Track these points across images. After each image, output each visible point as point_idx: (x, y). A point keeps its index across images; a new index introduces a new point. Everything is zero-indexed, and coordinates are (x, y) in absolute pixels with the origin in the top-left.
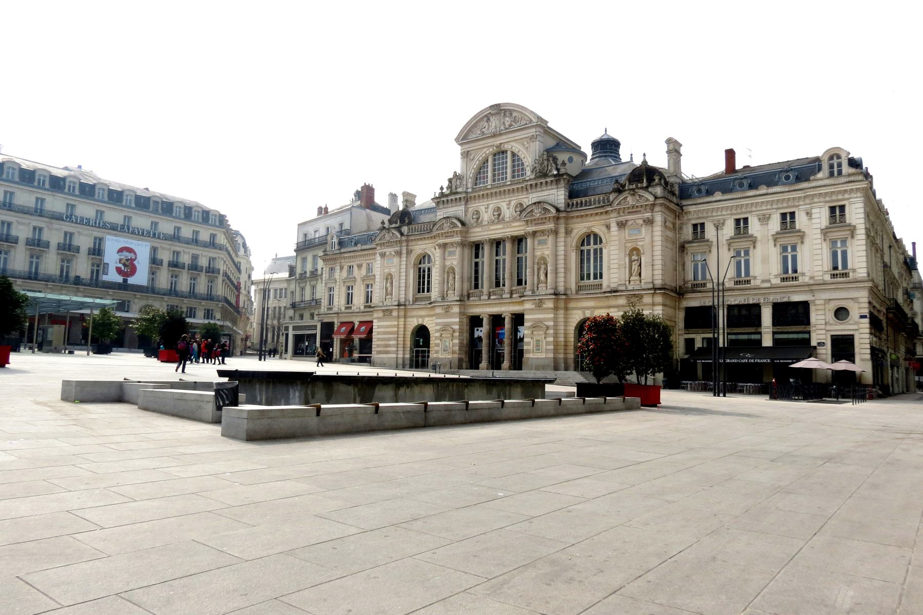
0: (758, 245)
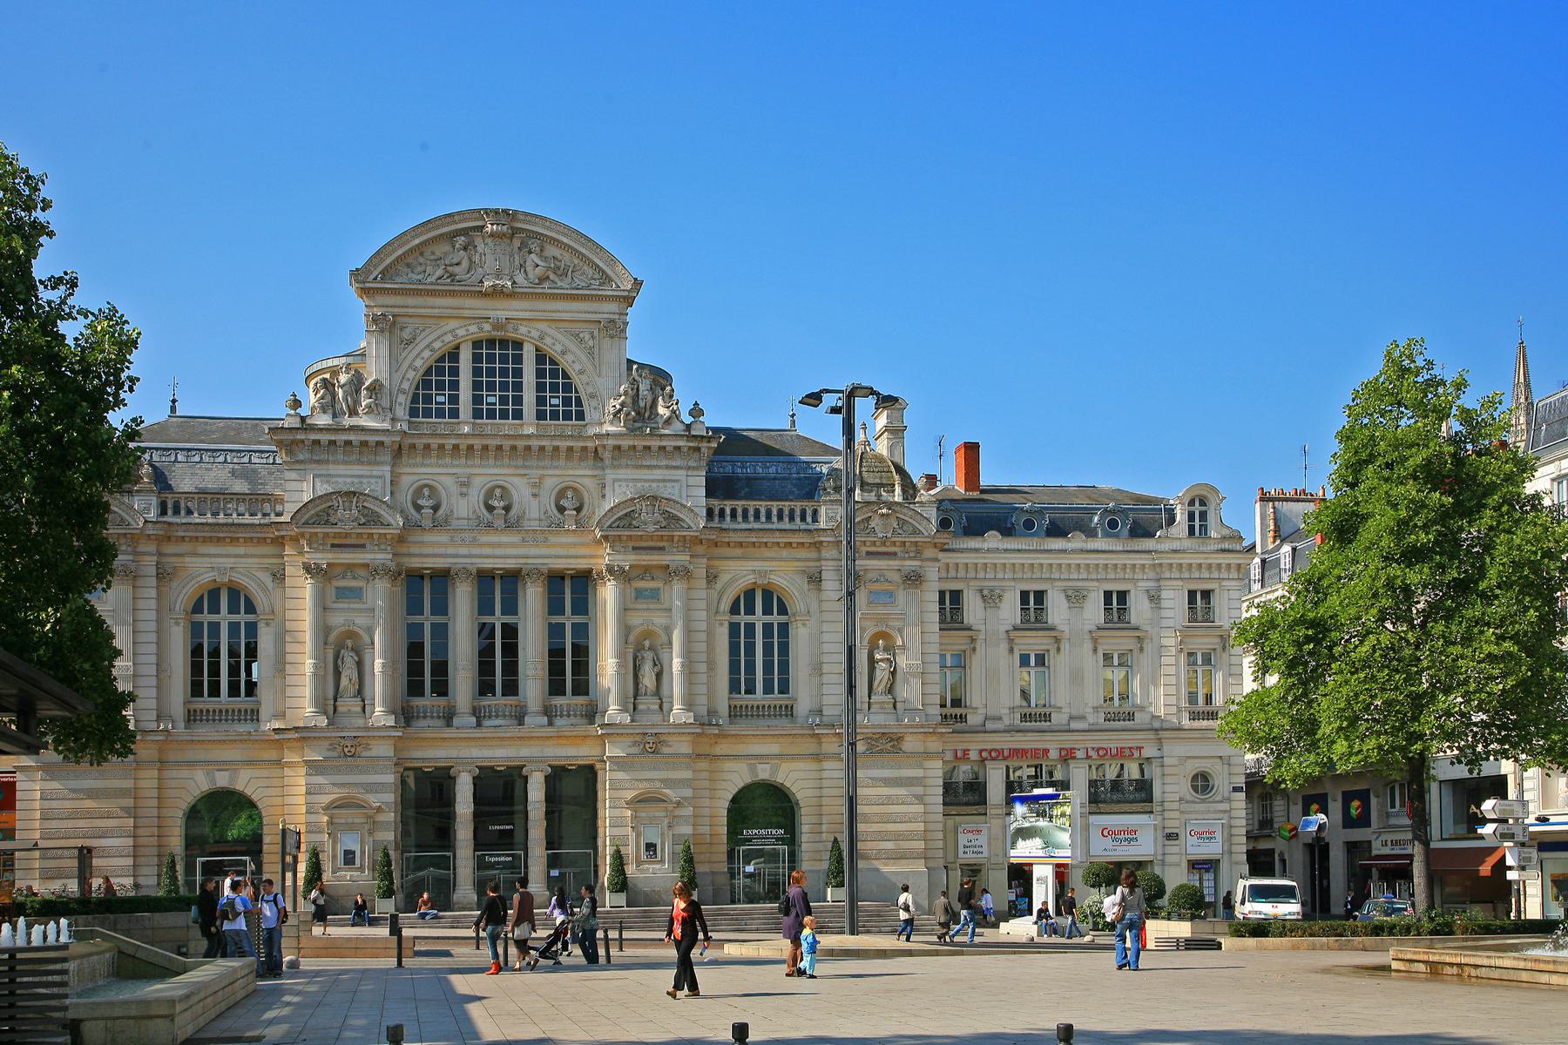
0: (1065, 646)
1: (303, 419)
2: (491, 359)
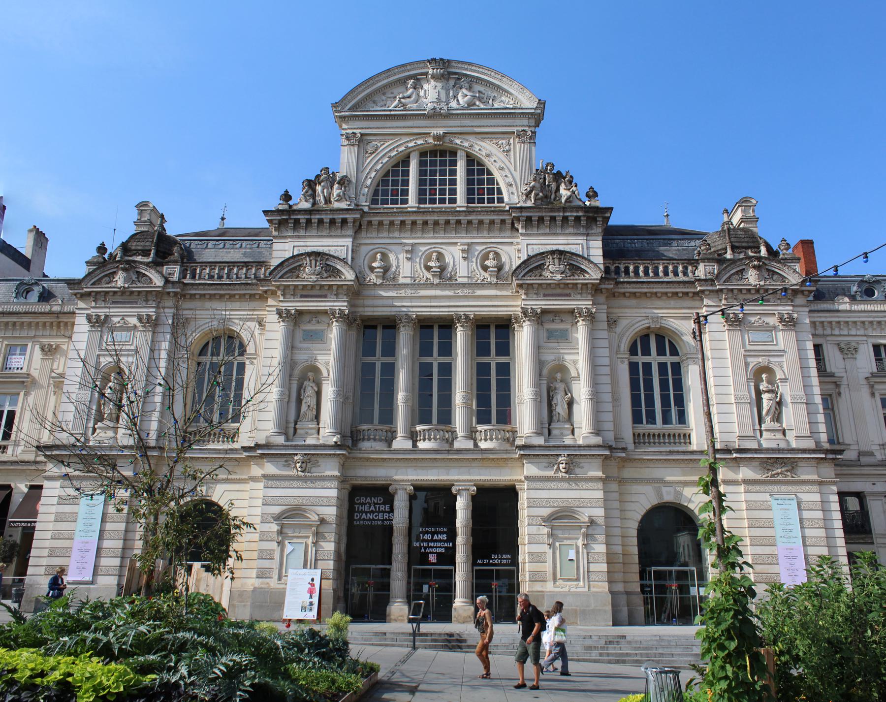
1: (290, 206)
2: (433, 163)
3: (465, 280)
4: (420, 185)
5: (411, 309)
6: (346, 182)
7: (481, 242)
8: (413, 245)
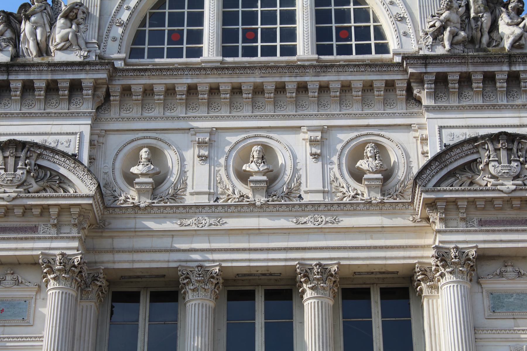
3: (318, 198)
4: (224, 23)
5: (210, 256)
6: (80, 16)
7: (348, 125)
8: (212, 132)
